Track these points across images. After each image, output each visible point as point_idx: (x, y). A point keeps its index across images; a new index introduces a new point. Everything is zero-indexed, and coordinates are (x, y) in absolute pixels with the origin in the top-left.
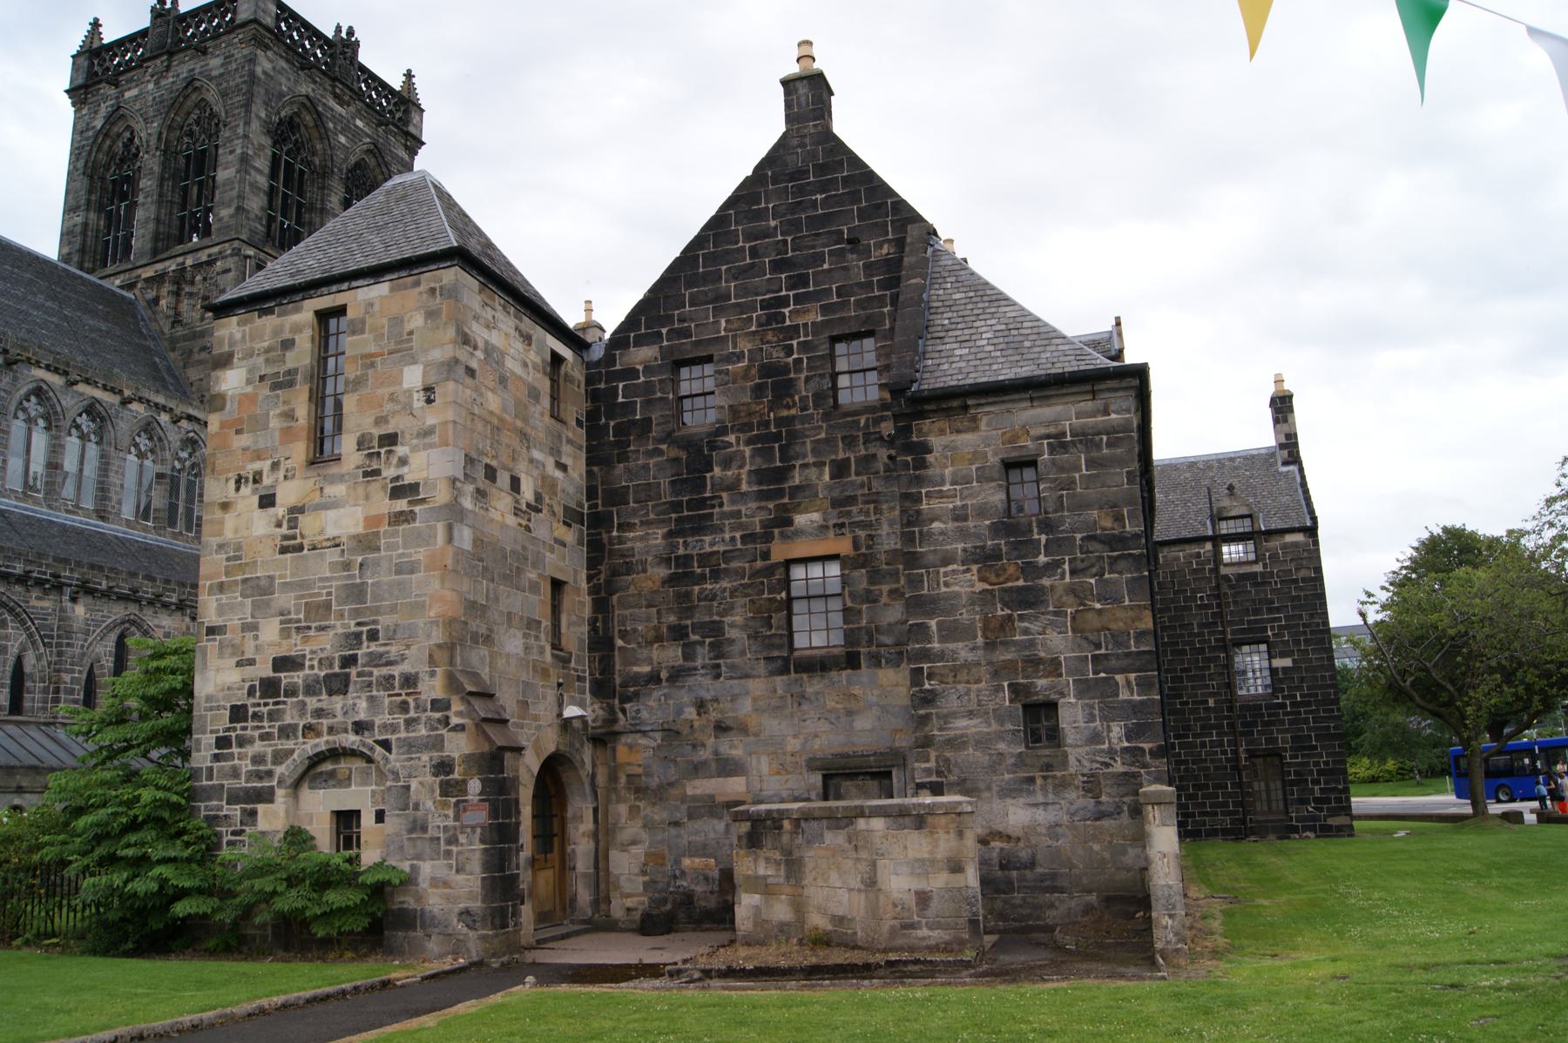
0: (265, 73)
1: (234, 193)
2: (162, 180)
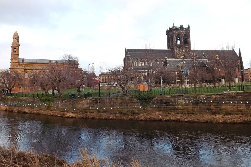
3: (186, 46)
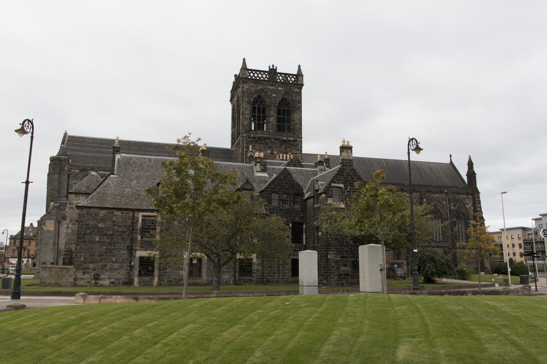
0: (247, 89)
3: (285, 138)
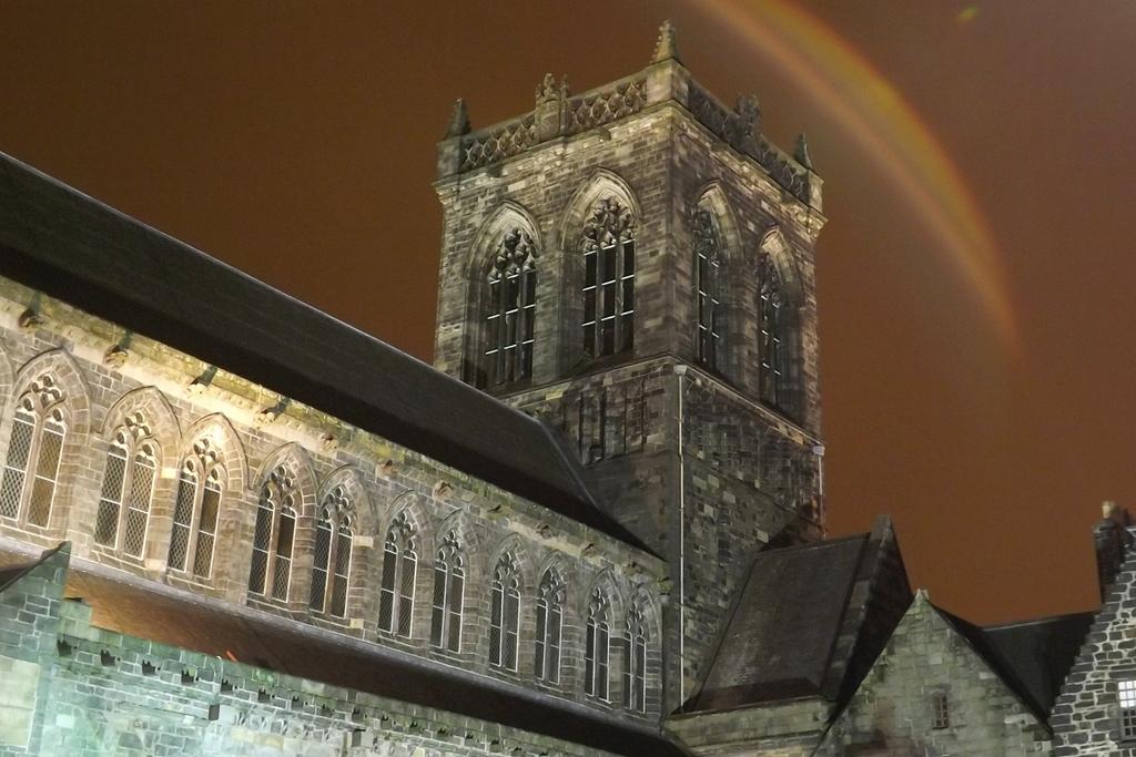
1: (659, 302)
2: (565, 285)
